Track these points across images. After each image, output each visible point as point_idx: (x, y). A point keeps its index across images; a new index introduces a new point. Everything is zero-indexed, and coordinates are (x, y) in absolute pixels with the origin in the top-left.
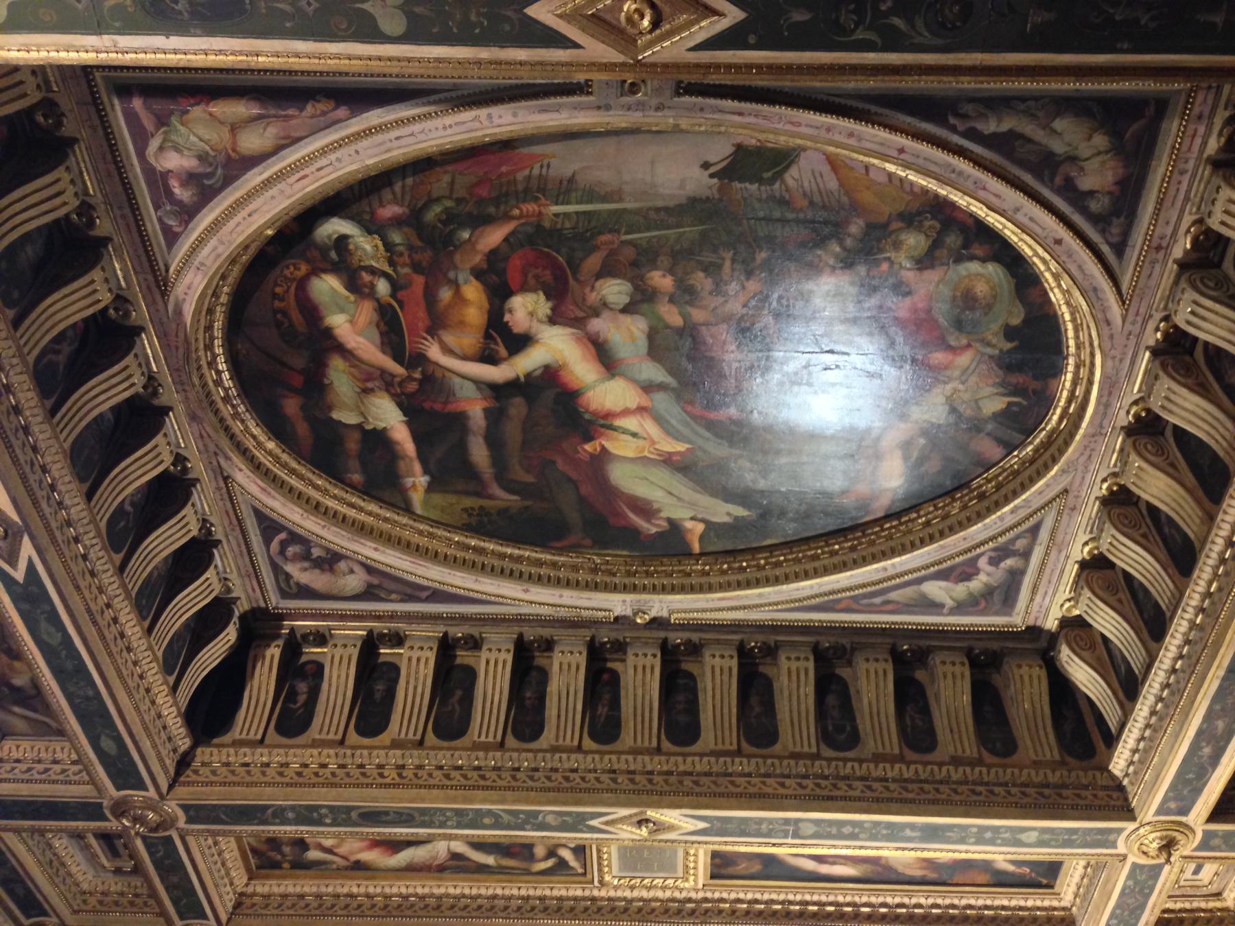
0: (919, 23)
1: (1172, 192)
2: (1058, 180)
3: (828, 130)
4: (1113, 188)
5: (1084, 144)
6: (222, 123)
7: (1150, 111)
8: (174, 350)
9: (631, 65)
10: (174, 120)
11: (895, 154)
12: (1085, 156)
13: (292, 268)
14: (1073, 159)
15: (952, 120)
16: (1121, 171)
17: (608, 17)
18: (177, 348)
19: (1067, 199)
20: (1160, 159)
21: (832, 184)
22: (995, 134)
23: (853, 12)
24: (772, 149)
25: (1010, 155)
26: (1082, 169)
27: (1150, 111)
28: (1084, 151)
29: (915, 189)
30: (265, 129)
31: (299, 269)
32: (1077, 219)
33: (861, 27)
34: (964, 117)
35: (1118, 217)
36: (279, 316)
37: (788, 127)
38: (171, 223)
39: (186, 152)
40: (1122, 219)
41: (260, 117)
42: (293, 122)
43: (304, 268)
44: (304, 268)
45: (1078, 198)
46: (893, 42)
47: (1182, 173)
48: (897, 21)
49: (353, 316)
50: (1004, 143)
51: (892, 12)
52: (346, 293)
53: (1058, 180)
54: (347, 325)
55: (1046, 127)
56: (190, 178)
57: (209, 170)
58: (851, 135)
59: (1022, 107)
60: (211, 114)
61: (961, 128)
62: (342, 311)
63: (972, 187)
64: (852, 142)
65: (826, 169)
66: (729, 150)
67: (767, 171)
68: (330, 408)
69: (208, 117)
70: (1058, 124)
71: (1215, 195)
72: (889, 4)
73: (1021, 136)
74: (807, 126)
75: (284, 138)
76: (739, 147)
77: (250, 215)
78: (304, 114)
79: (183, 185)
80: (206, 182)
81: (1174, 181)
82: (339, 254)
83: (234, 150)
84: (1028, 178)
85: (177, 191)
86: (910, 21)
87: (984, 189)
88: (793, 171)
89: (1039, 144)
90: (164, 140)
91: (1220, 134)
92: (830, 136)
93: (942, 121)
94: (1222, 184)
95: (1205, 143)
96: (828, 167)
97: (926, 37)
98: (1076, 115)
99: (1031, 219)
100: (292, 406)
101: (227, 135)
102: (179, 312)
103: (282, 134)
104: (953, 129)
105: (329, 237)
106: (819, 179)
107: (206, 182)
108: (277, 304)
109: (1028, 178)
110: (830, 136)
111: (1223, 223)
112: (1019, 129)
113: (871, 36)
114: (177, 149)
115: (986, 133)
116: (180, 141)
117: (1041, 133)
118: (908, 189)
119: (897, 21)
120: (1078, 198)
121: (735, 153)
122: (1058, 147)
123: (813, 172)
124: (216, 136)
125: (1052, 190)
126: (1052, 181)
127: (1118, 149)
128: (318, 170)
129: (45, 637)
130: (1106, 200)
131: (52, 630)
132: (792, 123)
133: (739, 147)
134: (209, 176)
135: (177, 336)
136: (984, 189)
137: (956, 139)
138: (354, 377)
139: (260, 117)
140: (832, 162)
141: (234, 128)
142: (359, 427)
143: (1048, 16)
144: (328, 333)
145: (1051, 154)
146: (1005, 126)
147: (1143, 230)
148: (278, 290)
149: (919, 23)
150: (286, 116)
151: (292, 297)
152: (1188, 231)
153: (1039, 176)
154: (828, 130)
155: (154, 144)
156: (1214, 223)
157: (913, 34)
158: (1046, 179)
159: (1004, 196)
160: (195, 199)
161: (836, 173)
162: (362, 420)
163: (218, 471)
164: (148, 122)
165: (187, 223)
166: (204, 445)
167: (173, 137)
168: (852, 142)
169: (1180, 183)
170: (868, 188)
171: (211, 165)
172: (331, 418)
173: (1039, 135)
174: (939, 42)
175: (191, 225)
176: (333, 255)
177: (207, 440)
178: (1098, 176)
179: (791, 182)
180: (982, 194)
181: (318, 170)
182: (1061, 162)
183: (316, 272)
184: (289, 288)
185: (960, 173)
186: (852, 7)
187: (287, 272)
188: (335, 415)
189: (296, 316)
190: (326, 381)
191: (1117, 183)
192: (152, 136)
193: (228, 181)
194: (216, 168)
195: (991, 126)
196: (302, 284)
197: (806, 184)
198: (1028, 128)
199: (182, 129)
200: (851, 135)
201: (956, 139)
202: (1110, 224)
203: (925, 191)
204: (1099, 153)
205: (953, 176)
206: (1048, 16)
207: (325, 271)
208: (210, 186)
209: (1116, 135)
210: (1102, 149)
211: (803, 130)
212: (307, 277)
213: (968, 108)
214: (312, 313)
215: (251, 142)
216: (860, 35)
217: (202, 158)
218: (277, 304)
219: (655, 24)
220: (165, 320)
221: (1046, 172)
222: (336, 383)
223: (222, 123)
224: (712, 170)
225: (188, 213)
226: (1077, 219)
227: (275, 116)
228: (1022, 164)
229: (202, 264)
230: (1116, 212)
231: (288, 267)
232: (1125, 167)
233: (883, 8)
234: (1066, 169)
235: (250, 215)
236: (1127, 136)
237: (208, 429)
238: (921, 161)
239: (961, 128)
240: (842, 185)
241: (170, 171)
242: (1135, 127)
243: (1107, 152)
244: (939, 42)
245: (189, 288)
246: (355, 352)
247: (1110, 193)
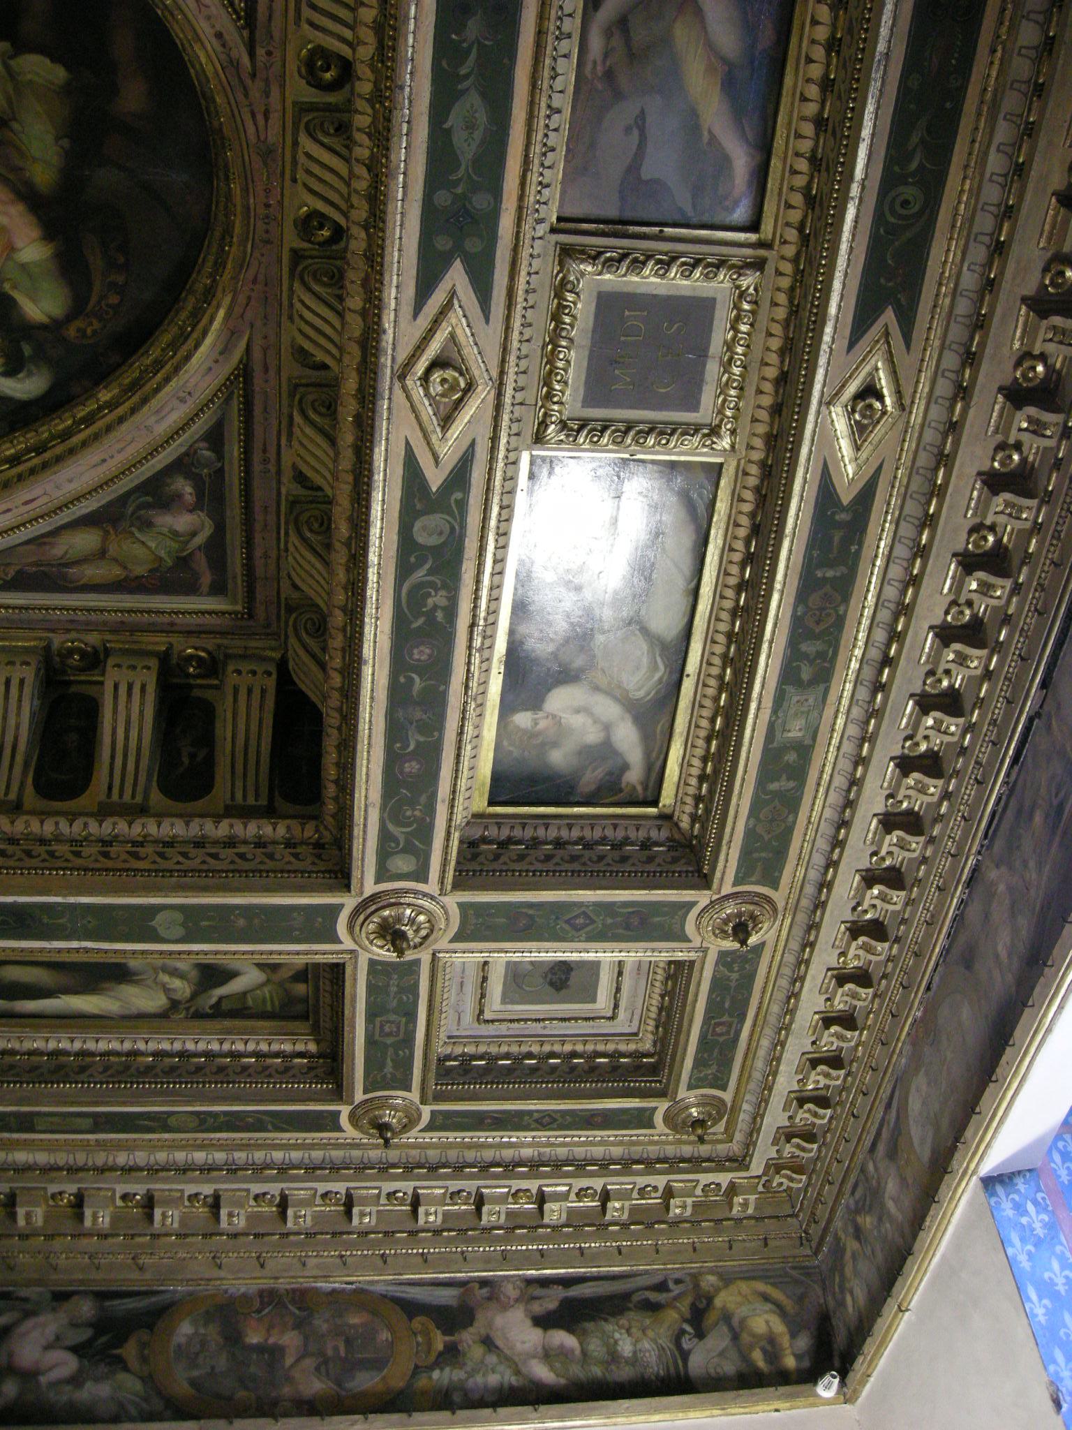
6: (116, 560)
8: (261, 277)
10: (170, 563)
13: (89, 331)
18: (255, 281)
30: (66, 553)
31: (79, 330)
36: (122, 260)
38: (207, 453)
39: (165, 530)
41: (67, 565)
42: (34, 559)
43: (71, 332)
44: (71, 332)
49: (9, 258)
52: (16, 295)
54: (19, 244)
56: (167, 503)
57: (142, 512)
60: (125, 568)
62: (23, 267)
68: (67, 90)
69: (129, 566)
75: (45, 543)
77: (104, 461)
78: (18, 568)
79: (179, 496)
80: (149, 499)
82: (20, 350)
83: (107, 533)
85: (189, 489)
90: (187, 542)
100: (133, 97)
101: (113, 550)
102: (232, 334)
103: (47, 547)
105: (30, 374)
107: (149, 499)
108: (120, 279)
114: (175, 534)
116: (169, 542)
124: (125, 547)
128: (9, 510)
129: (482, 117)
131: (459, 138)
134: (148, 506)
135: (249, 298)
138: (18, 150)
139: (67, 565)
141: (102, 554)
142: (21, 47)
144: (50, 231)
148: (114, 299)
150: (38, 565)
151: (97, 286)
155: (200, 540)
160: (169, 481)
162: (12, 62)
163: (258, 34)
164: (201, 563)
165: (187, 454)
166: (267, 94)
167: (175, 545)
171: (139, 518)
172: (68, 68)
175: (183, 450)
176: (27, 350)
177: (259, 110)
181: (9, 510)
183: (56, 326)
184: (99, 302)
187: (96, 325)
188: (59, 74)
189: (96, 262)
190: (65, 143)
192: (199, 548)
193: (123, 499)
194: (133, 514)
196: (78, 308)
199: (163, 554)
207: (43, 327)
208: (147, 494)
212: (69, 318)
214: (70, 265)
215: (86, 540)
217: (148, 525)
218: (120, 279)
220: (258, 323)
222: (50, 138)
223: (116, 560)
225: (180, 466)
227: (52, 566)
229: (183, 401)
231: (94, 332)
235: (104, 461)
237: (251, 130)
241: (191, 511)
245: (210, 369)
246: (11, 196)
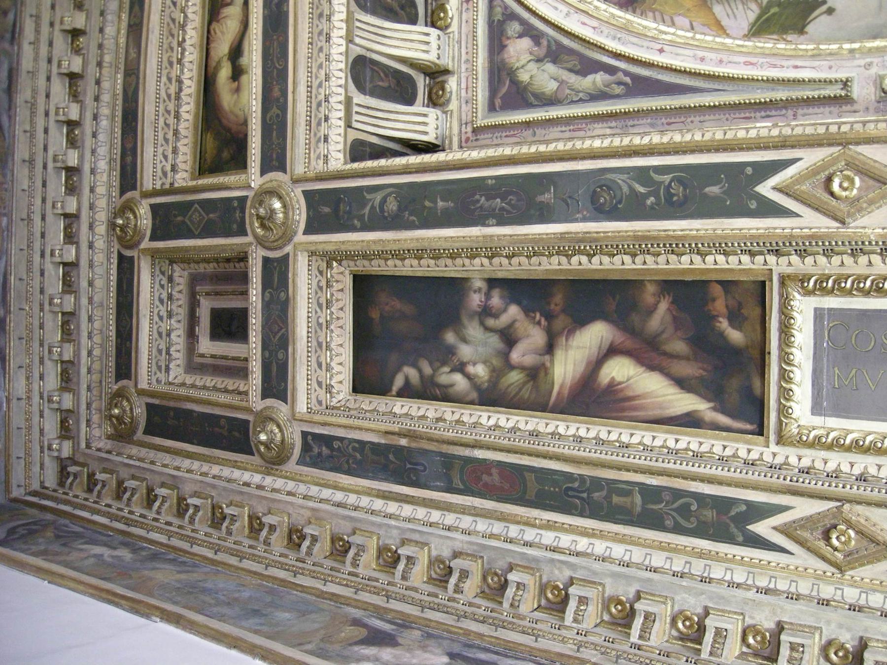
0: (625, 189)
1: (470, 45)
2: (544, 43)
3: (721, 61)
4: (508, 42)
5: (533, 73)
7: (498, 102)
9: (851, 144)
11: (666, 48)
12: (531, 63)
14: (539, 60)
15: (628, 80)
16: (506, 56)
17: (871, 182)
19: (536, 29)
20: (483, 68)
21: (718, 9)
22: (596, 72)
23: (674, 195)
24: (772, 33)
25: (581, 57)
26: (531, 53)
27: (498, 102)
28: (532, 66)
29: (650, 14)
32: (526, 15)
33: (667, 183)
34: (619, 83)
35: (499, 20)
37: (754, 60)
40: (496, 19)
45: (529, 31)
46: (642, 174)
47: (467, 61)
48: (642, 190)
50: (588, 67)
51: (646, 196)
53: (544, 43)
55: (562, 82)
58: (702, 59)
59: (581, 95)
61: (620, 75)
63: (603, 28)
64: (700, 54)
65: (725, 22)
66: (809, 28)
67: (774, 14)
70: (553, 86)
71: (439, 52)
72: (649, 202)
73: (577, 73)
74: (740, 63)
76: (801, 31)
81: (470, 54)
84: (566, 41)
86: (631, 188)
87: (594, 28)
88: (752, 16)
89: (562, 68)
91: (451, 92)
92: (719, 56)
93: (635, 78)
94: (437, 61)
95: (459, 84)
96: (723, 23)
97: (619, 178)
98: (543, 93)
99: (556, 9)
104: (626, 73)
106: (730, 12)
109: (566, 41)
110: (719, 56)
111: (427, 34)
112: (580, 78)
113: (657, 178)
115: (602, 73)
117: (564, 78)
118: (657, 13)
119: (642, 190)
120: (529, 31)
121: (804, 26)
122: (550, 68)
123: (735, 17)
125: (547, 35)
126: (548, 41)
127: (512, 73)
130: (510, 33)
132: (751, 64)
133: (801, 31)
136: (594, 28)
137: (622, 65)
140: (721, 30)
143: (540, 198)
145: (554, 62)
146: (590, 78)
147: (480, 13)
149: (625, 189)
152: (452, 19)
153: (559, 44)
154: (721, 61)
156: (434, 32)
157: (628, 181)
158: (553, 43)
159: (579, 24)
161: (716, 18)
168: (700, 54)
169: (467, 53)
170: (688, 10)
173: (565, 75)
174: (610, 176)
178: (519, 50)
179: (754, 6)
180: (595, 23)
182: (545, 57)
185: (614, 38)
186: (675, 198)
191: (506, 46)
195: (599, 79)
197: (740, 6)
198: (573, 79)
200: (702, 59)
201: (622, 65)
202: (503, 14)
203: (643, 14)
204: (523, 67)
205: (619, 36)
206: (540, 198)
209: (515, 82)
210: (522, 70)
211: (742, 59)
213: (618, 90)
216: (667, 178)
219: (829, 180)
221: (554, 48)
224: (824, 8)
226: (526, 15)
228: (571, 52)
230: (501, 23)
232: (503, 61)
233: (652, 199)
234: (541, 52)
236: (508, 82)
238: (646, 44)
239: (620, 75)
240: (710, 9)
242: (504, 90)
243: (517, 69)
244: (610, 176)
247: (508, 38)
